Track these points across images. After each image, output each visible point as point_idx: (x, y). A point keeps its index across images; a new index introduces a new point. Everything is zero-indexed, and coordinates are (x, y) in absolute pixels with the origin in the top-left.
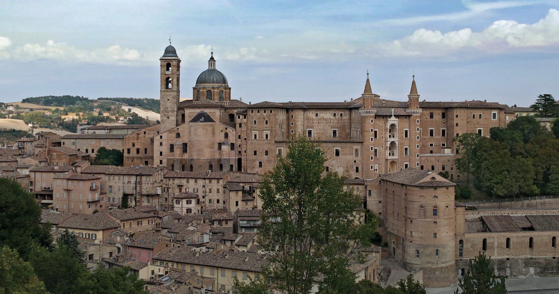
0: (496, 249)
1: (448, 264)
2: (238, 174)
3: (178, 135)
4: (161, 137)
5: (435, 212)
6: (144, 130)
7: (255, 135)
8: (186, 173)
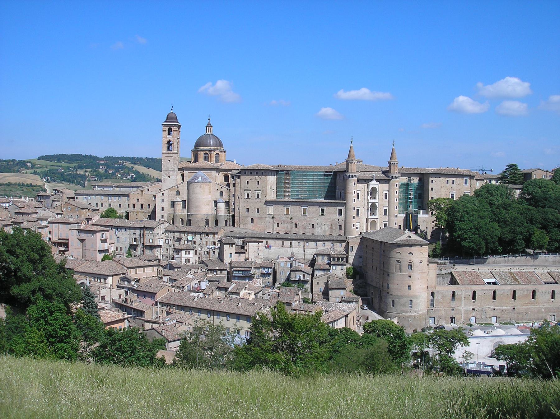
0: (463, 301)
1: (421, 313)
2: (232, 228)
3: (178, 193)
4: (163, 194)
5: (410, 266)
7: (248, 194)
8: (186, 228)
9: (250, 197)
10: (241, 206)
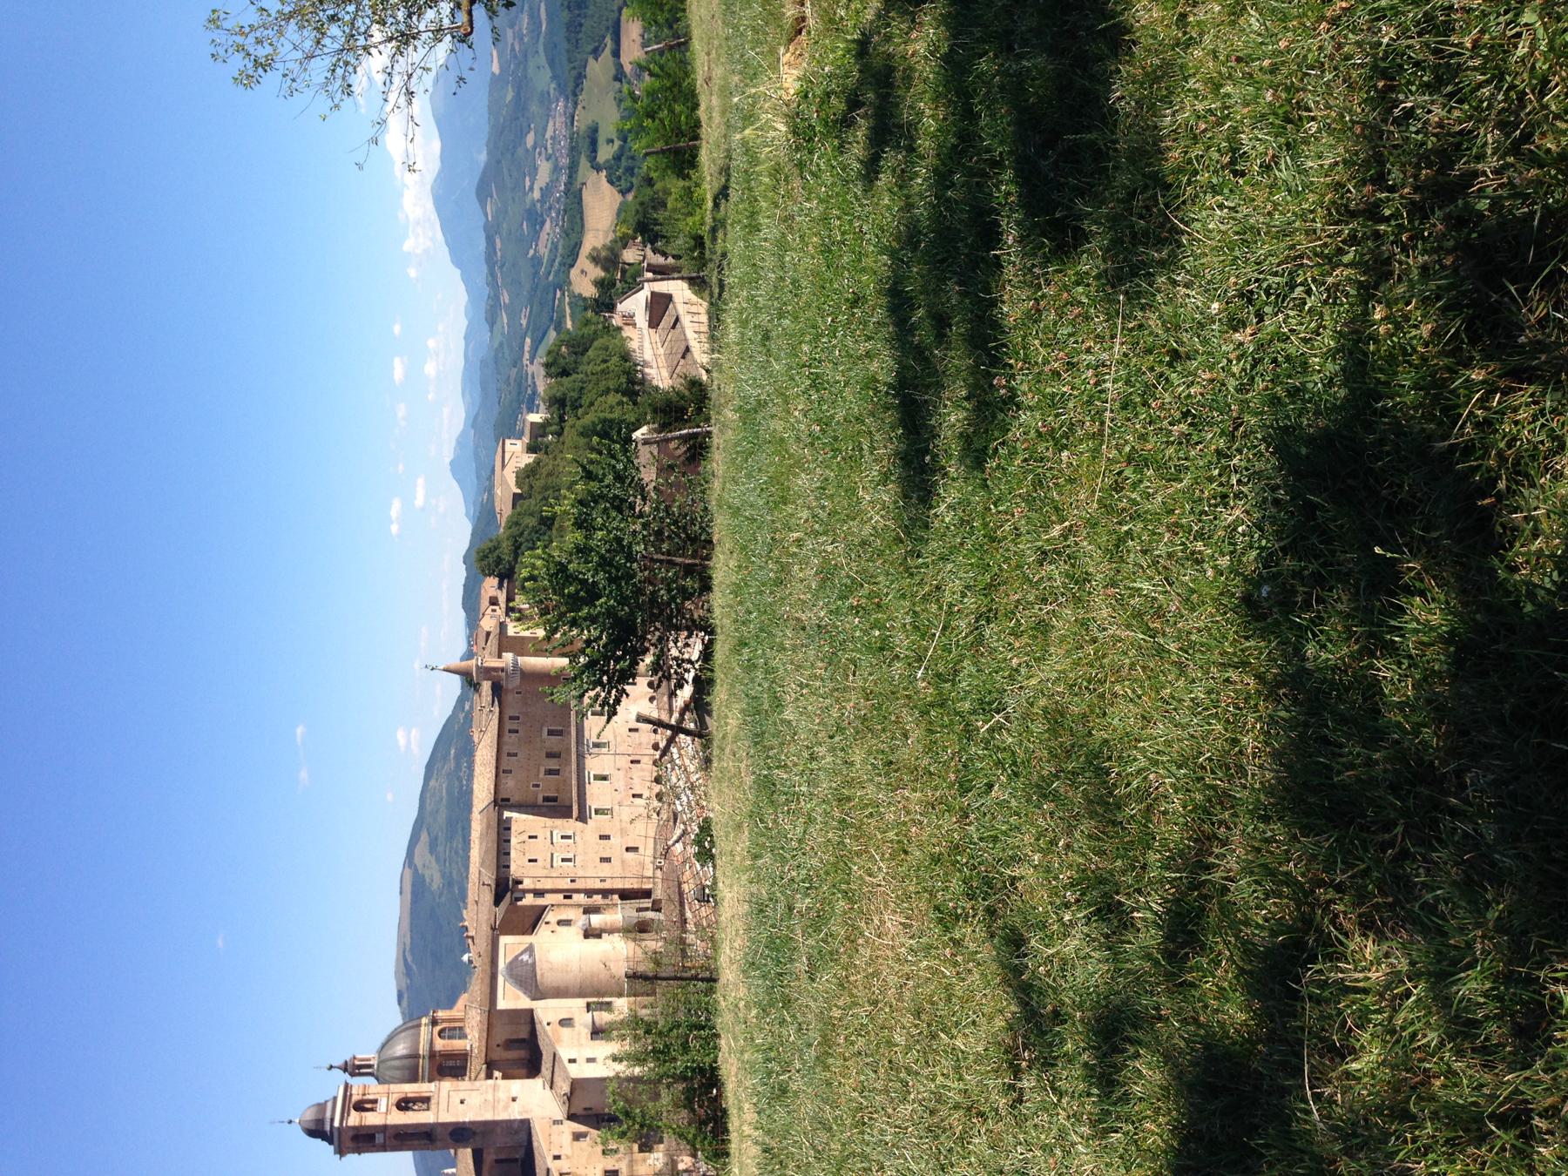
3: (566, 1022)
4: (572, 1061)
6: (549, 1160)
9: (570, 856)
10: (592, 874)
